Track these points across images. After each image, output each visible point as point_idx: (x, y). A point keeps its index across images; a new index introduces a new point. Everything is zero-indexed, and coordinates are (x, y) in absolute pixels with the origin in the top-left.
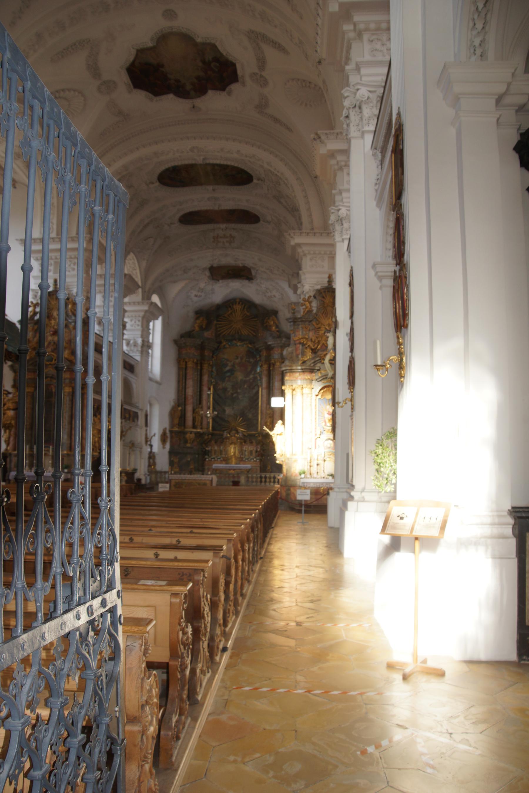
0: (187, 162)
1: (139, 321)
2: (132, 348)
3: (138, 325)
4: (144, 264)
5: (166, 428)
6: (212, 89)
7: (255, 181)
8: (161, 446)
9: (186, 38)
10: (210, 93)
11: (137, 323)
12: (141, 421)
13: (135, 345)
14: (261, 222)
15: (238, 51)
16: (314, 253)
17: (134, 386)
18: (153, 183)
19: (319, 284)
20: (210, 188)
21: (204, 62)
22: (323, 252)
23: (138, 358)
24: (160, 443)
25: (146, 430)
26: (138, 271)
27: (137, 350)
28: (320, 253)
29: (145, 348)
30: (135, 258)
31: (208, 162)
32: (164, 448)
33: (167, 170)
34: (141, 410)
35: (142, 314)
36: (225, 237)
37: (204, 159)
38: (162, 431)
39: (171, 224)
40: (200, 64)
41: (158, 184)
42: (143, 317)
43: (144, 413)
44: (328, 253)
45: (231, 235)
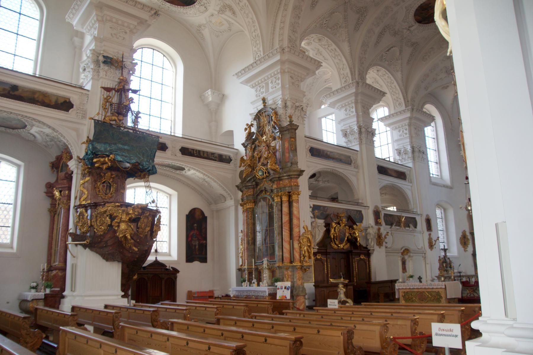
1: (406, 130)
2: (404, 156)
3: (406, 134)
4: (399, 75)
5: (464, 231)
8: (463, 249)
11: (405, 131)
12: (421, 224)
13: (406, 153)
17: (409, 193)
23: (410, 165)
24: (461, 246)
25: (430, 235)
26: (395, 84)
27: (408, 157)
29: (417, 154)
30: (387, 72)
32: (465, 251)
34: (421, 215)
35: (407, 122)
38: (460, 234)
39: (409, 27)
42: (410, 125)
43: (424, 217)
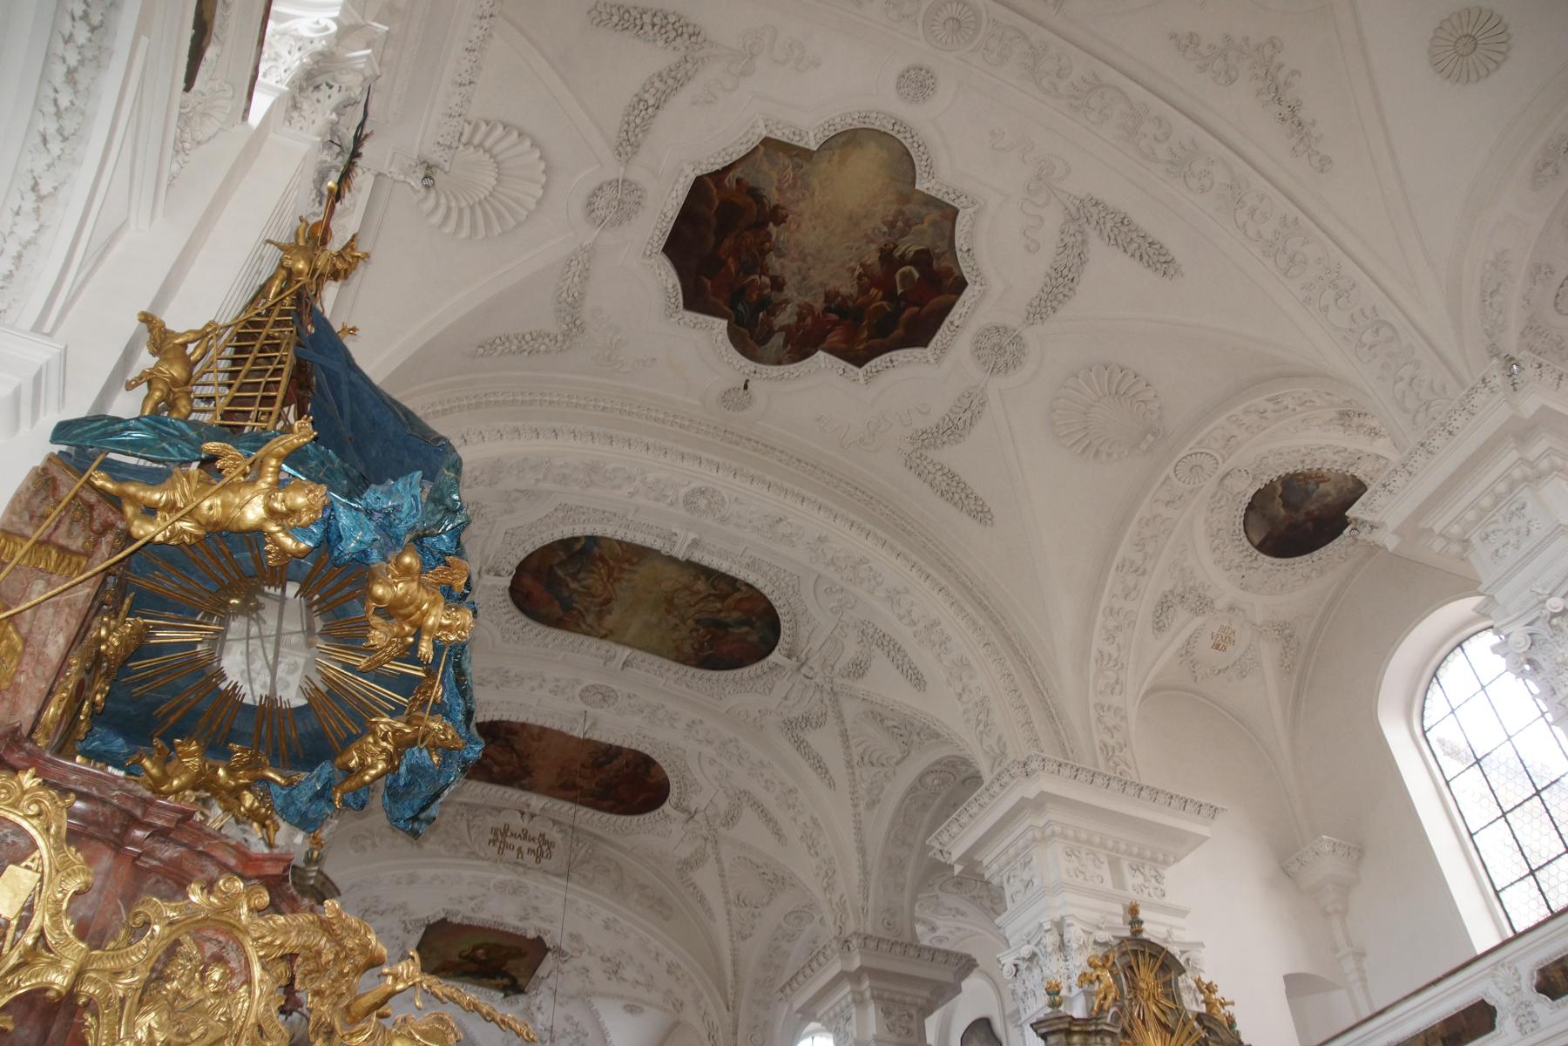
0: (639, 538)
6: (831, 351)
7: (775, 657)
9: (901, 161)
10: (821, 356)
14: (667, 807)
15: (999, 256)
16: (1077, 839)
18: (498, 574)
19: (1108, 928)
20: (624, 653)
21: (886, 255)
22: (1097, 840)
28: (1089, 842)
31: (696, 557)
33: (566, 544)
36: (525, 835)
37: (695, 543)
40: (872, 258)
41: (506, 581)
44: (1110, 844)
45: (542, 835)
